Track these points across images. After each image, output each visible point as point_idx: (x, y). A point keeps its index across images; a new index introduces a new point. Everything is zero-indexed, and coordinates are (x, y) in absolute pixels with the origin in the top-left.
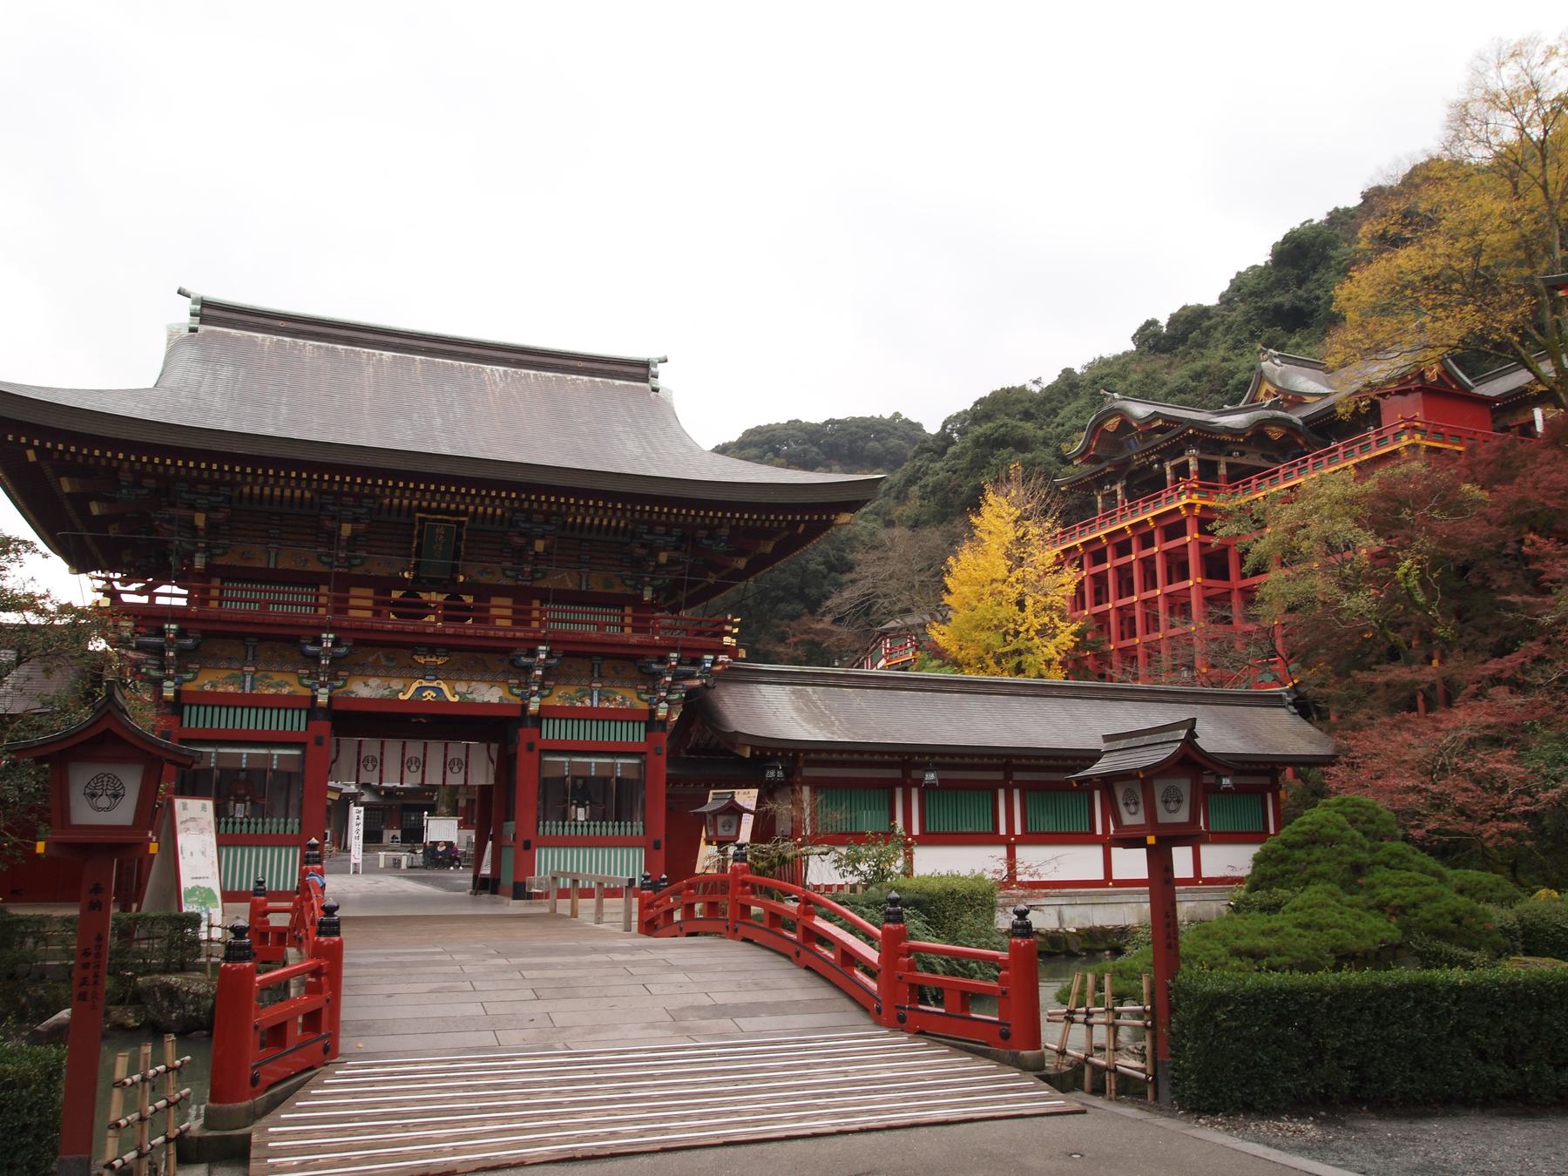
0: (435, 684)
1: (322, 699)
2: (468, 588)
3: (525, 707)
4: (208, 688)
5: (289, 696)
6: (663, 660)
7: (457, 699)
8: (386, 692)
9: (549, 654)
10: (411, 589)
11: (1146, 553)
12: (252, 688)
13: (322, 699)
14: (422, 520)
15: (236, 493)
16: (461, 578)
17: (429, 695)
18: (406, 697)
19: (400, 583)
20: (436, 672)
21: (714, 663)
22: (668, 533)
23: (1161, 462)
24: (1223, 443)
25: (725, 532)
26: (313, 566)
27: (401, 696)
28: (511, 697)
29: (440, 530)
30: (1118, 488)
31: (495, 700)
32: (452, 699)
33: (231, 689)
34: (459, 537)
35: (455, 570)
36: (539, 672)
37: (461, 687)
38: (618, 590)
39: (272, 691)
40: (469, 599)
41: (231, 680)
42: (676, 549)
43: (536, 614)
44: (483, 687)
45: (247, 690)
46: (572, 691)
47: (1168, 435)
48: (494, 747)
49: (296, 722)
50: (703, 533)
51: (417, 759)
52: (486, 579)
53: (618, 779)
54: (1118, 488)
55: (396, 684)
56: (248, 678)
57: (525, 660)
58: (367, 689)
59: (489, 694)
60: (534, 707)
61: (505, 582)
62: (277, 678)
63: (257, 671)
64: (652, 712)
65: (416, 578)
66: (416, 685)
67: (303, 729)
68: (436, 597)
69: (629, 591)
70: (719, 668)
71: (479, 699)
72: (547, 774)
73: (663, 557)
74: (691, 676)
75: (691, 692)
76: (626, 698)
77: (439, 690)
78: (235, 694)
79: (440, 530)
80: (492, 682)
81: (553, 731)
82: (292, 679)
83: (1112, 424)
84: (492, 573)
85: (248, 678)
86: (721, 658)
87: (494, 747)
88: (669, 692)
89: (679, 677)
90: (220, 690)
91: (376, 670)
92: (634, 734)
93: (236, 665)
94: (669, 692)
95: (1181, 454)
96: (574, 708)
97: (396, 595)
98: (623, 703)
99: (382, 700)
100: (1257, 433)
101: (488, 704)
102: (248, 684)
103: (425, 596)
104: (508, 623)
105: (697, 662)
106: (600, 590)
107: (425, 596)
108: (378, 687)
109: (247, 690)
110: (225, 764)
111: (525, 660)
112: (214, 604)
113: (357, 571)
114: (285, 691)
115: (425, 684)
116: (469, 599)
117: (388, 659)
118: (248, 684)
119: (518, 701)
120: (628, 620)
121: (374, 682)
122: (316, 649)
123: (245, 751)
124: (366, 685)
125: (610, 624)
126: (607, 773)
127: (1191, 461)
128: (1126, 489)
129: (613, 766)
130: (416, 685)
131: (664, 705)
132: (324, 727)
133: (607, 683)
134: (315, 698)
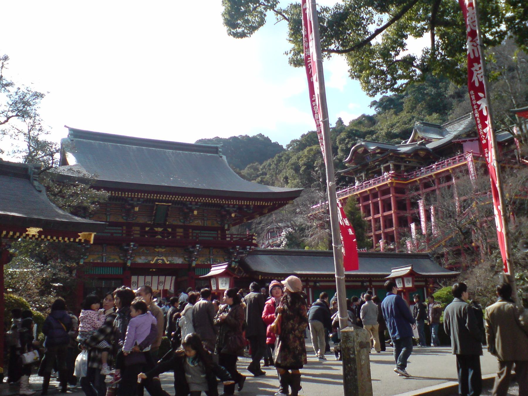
1: (129, 264)
2: (170, 226)
3: (190, 265)
4: (91, 261)
5: (117, 263)
6: (234, 248)
7: (168, 263)
9: (134, 246)
10: (152, 227)
11: (375, 200)
13: (129, 264)
16: (167, 223)
17: (160, 262)
18: (153, 262)
19: (148, 225)
20: (162, 254)
21: (250, 249)
22: (234, 207)
23: (379, 165)
24: (402, 158)
26: (121, 220)
27: (152, 262)
30: (363, 174)
31: (180, 263)
33: (99, 261)
34: (168, 210)
35: (166, 220)
36: (130, 252)
37: (170, 258)
38: (216, 225)
39: (111, 262)
40: (170, 230)
43: (190, 234)
44: (176, 258)
47: (383, 155)
48: (174, 278)
51: (149, 282)
52: (175, 223)
54: (363, 174)
55: (150, 258)
56: (104, 258)
57: (191, 249)
58: (140, 260)
59: (179, 261)
60: (194, 264)
61: (181, 224)
62: (112, 257)
66: (156, 258)
68: (160, 229)
73: (233, 215)
74: (242, 253)
77: (163, 260)
78: (100, 263)
80: (179, 257)
83: (360, 150)
86: (253, 247)
87: (174, 278)
88: (235, 258)
89: (239, 253)
90: (96, 261)
91: (143, 254)
94: (235, 258)
95: (387, 162)
96: (204, 264)
97: (147, 229)
100: (415, 153)
103: (156, 229)
105: (244, 248)
107: (156, 229)
109: (104, 261)
111: (191, 249)
113: (133, 221)
114: (116, 261)
116: (170, 230)
119: (186, 263)
121: (143, 258)
122: (127, 248)
127: (391, 166)
128: (366, 175)
130: (156, 258)
134: (126, 264)
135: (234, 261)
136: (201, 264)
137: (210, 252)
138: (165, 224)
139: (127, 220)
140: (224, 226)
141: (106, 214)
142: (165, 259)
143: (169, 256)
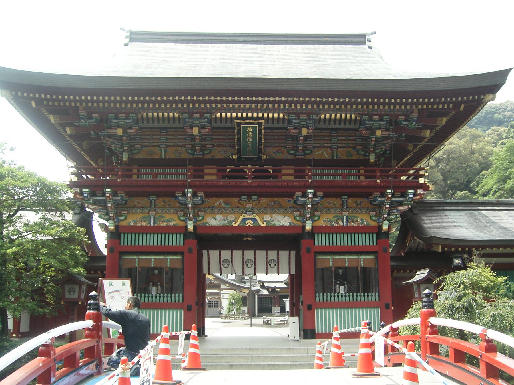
0: (252, 216)
1: (190, 227)
2: (268, 162)
3: (304, 227)
4: (132, 224)
5: (174, 227)
7: (265, 224)
8: (226, 222)
12: (154, 223)
13: (190, 227)
14: (239, 124)
15: (140, 117)
17: (249, 223)
18: (237, 225)
19: (230, 162)
21: (415, 195)
25: (415, 115)
27: (234, 224)
28: (296, 222)
29: (249, 129)
31: (287, 224)
32: (262, 225)
33: (144, 224)
34: (260, 131)
37: (267, 217)
38: (355, 157)
39: (165, 224)
41: (144, 219)
42: (387, 130)
45: (152, 224)
46: (331, 217)
49: (178, 240)
50: (402, 118)
51: (251, 260)
52: (278, 156)
53: (361, 267)
55: (231, 217)
56: (152, 218)
58: (215, 221)
59: (283, 221)
61: (289, 157)
62: (167, 217)
63: (156, 213)
64: (380, 227)
65: (239, 158)
66: (242, 218)
67: (182, 244)
69: (362, 158)
70: (418, 197)
71: (277, 224)
72: (319, 265)
74: (401, 204)
75: (403, 215)
76: (363, 219)
77: (254, 220)
78: (146, 227)
79: (249, 129)
80: (285, 215)
81: (321, 241)
82: (175, 217)
84: (282, 152)
85: (152, 218)
86: (419, 191)
88: (389, 215)
90: (139, 225)
91: (219, 209)
92: (370, 241)
93: (145, 211)
98: (362, 223)
99: (223, 227)
101: (283, 227)
102: (152, 221)
104: (292, 178)
105: (404, 195)
106: (344, 157)
108: (221, 219)
110: (144, 265)
112: (135, 177)
114: (172, 224)
115: (247, 216)
117: (226, 203)
118: (152, 221)
119: (300, 224)
120: (362, 172)
121: (219, 217)
123: (153, 257)
124: (215, 219)
125: (351, 175)
126: (354, 264)
129: (358, 260)
131: (386, 222)
132: (193, 243)
133: (351, 211)
135: (386, 219)
136: (326, 227)
137: (342, 205)
138: (260, 158)
139: (193, 154)
140: (368, 156)
141: (159, 146)
142: (257, 218)
143: (266, 213)
